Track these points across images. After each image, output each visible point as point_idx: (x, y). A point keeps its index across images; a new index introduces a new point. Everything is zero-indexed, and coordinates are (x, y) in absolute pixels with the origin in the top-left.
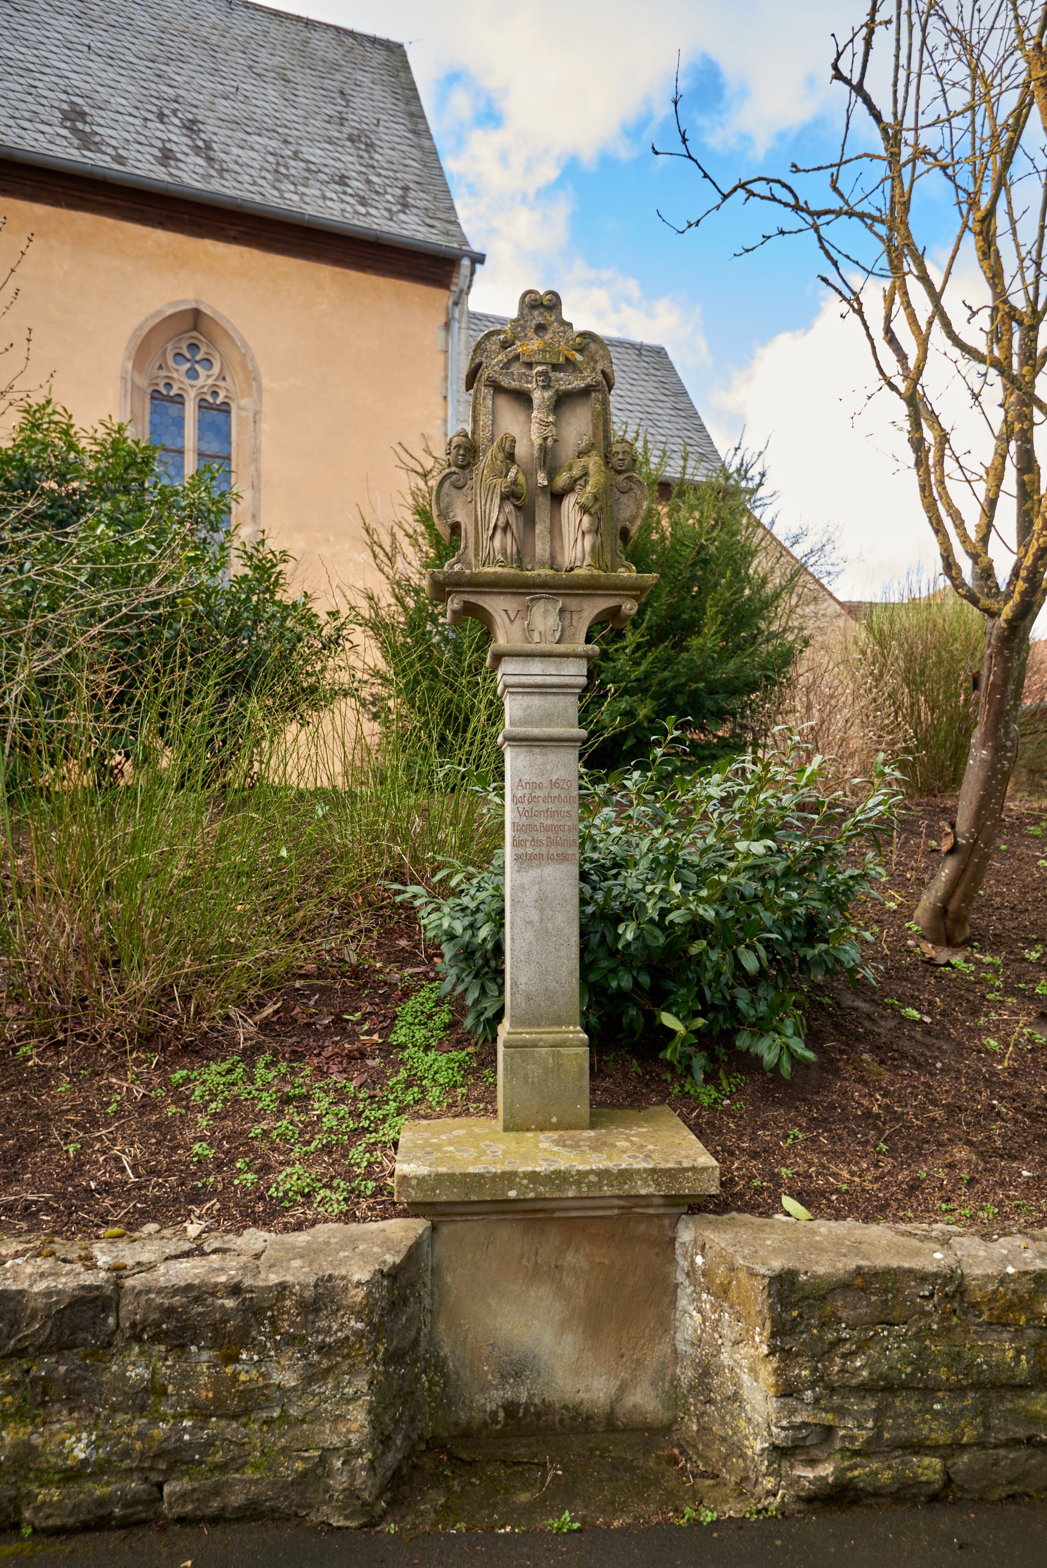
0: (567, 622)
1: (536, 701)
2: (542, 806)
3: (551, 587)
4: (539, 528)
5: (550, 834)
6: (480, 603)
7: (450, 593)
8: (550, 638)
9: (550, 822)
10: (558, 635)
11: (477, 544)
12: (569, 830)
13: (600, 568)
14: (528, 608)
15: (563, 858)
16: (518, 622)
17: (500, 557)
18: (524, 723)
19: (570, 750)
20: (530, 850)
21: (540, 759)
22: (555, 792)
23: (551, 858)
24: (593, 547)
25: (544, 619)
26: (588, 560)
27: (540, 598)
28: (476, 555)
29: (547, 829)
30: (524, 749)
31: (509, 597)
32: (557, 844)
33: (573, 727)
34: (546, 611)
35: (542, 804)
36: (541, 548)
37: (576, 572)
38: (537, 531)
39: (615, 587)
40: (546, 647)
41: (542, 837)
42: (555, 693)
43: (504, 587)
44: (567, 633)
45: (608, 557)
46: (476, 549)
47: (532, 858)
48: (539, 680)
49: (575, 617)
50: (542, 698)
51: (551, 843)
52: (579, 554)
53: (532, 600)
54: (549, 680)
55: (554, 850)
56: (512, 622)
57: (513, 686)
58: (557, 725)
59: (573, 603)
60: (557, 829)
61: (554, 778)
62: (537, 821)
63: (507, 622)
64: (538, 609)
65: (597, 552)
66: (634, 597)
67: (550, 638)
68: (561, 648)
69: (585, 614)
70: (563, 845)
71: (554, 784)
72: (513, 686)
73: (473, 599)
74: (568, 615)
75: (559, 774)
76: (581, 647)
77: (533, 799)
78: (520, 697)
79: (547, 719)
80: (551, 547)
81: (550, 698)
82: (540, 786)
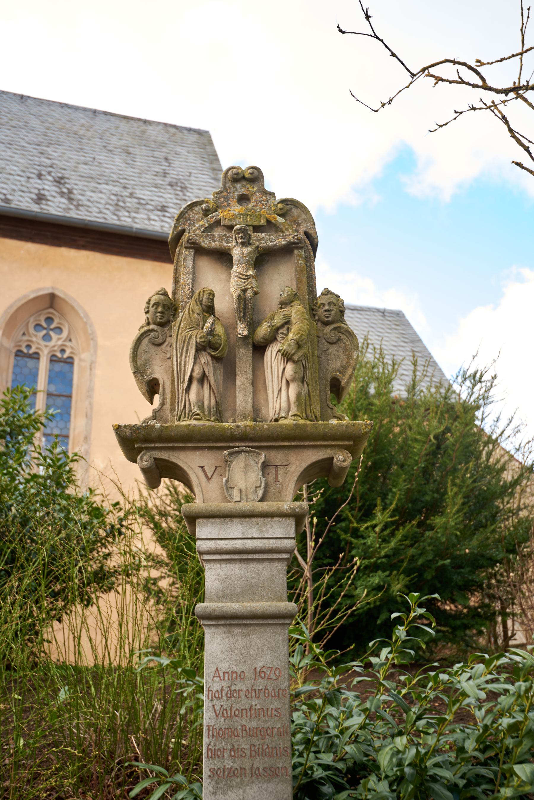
0: (271, 478)
1: (236, 570)
2: (245, 703)
3: (252, 440)
4: (240, 380)
5: (256, 742)
6: (173, 460)
7: (140, 450)
8: (251, 496)
9: (254, 724)
10: (260, 492)
11: (173, 399)
12: (279, 734)
13: (307, 418)
14: (227, 463)
15: (271, 774)
16: (215, 479)
17: (196, 410)
18: (222, 597)
19: (279, 629)
20: (229, 764)
21: (241, 641)
22: (260, 684)
23: (255, 774)
24: (299, 396)
25: (245, 475)
26: (294, 410)
27: (242, 452)
28: (172, 410)
29: (251, 733)
30: (222, 630)
31: (206, 452)
32: (263, 753)
33: (280, 600)
34: (246, 466)
35: (244, 700)
36: (242, 400)
37: (280, 422)
38: (238, 383)
39: (324, 437)
40: (246, 506)
41: (245, 745)
42: (259, 560)
43: (200, 441)
44: (271, 490)
45: (317, 408)
46: (172, 404)
47: (231, 773)
48: (238, 545)
49: (281, 471)
50: (244, 566)
51: (256, 752)
52: (284, 405)
53: (230, 454)
54: (250, 544)
55: (260, 763)
56: (209, 479)
57: (208, 553)
58: (262, 599)
59: (277, 457)
60: (263, 732)
61: (259, 665)
62: (238, 723)
63: (203, 479)
64: (238, 464)
65: (303, 402)
66: (347, 448)
67: (251, 496)
68: (264, 507)
69: (292, 469)
70: (271, 756)
71: (258, 674)
72: (208, 553)
73: (165, 455)
74: (273, 470)
75: (265, 660)
76: (287, 504)
77: (232, 694)
78: (217, 566)
79: (249, 591)
80: (254, 399)
81: (253, 566)
82: (241, 676)
